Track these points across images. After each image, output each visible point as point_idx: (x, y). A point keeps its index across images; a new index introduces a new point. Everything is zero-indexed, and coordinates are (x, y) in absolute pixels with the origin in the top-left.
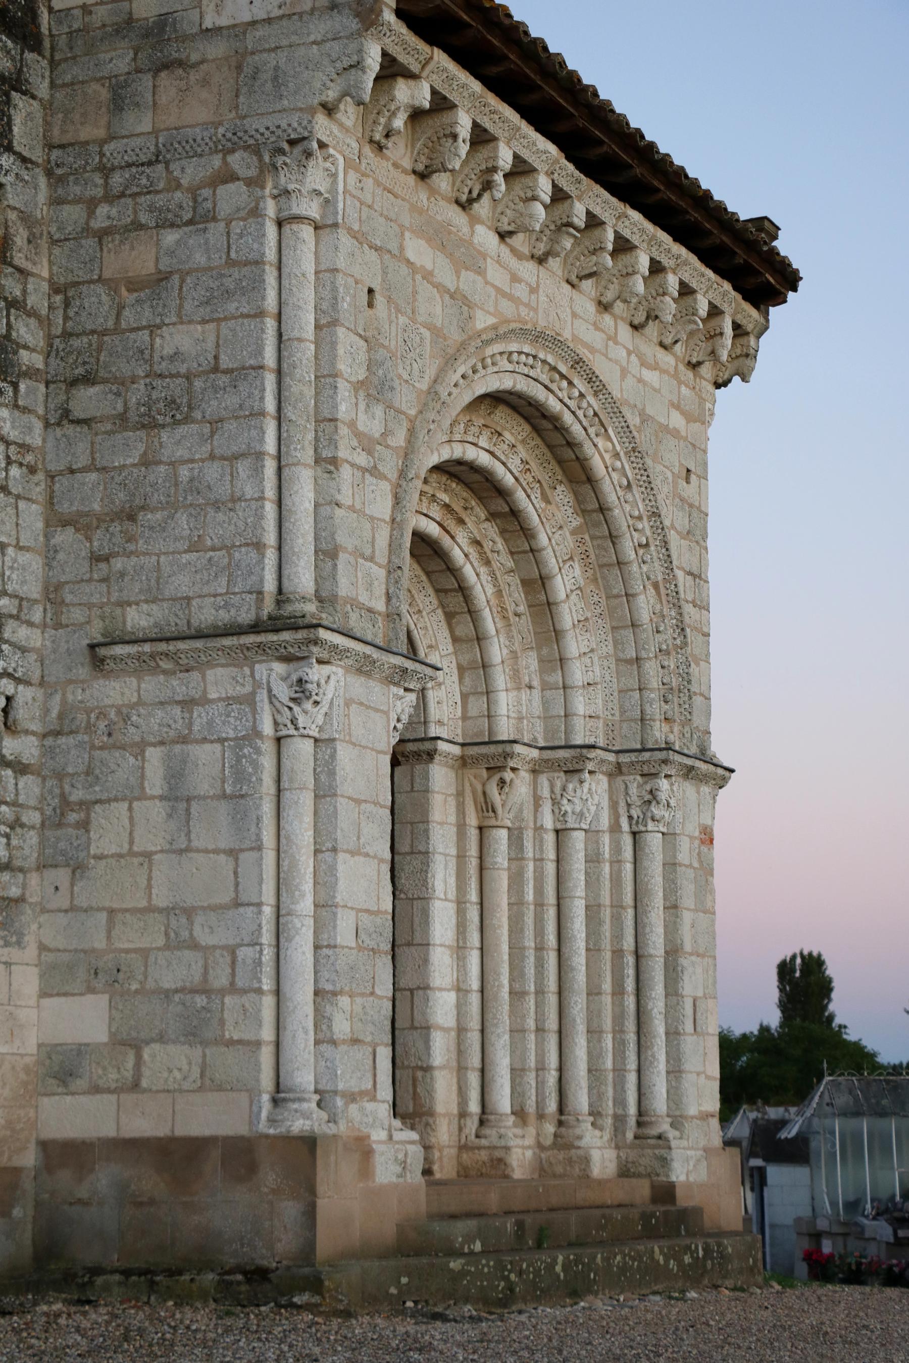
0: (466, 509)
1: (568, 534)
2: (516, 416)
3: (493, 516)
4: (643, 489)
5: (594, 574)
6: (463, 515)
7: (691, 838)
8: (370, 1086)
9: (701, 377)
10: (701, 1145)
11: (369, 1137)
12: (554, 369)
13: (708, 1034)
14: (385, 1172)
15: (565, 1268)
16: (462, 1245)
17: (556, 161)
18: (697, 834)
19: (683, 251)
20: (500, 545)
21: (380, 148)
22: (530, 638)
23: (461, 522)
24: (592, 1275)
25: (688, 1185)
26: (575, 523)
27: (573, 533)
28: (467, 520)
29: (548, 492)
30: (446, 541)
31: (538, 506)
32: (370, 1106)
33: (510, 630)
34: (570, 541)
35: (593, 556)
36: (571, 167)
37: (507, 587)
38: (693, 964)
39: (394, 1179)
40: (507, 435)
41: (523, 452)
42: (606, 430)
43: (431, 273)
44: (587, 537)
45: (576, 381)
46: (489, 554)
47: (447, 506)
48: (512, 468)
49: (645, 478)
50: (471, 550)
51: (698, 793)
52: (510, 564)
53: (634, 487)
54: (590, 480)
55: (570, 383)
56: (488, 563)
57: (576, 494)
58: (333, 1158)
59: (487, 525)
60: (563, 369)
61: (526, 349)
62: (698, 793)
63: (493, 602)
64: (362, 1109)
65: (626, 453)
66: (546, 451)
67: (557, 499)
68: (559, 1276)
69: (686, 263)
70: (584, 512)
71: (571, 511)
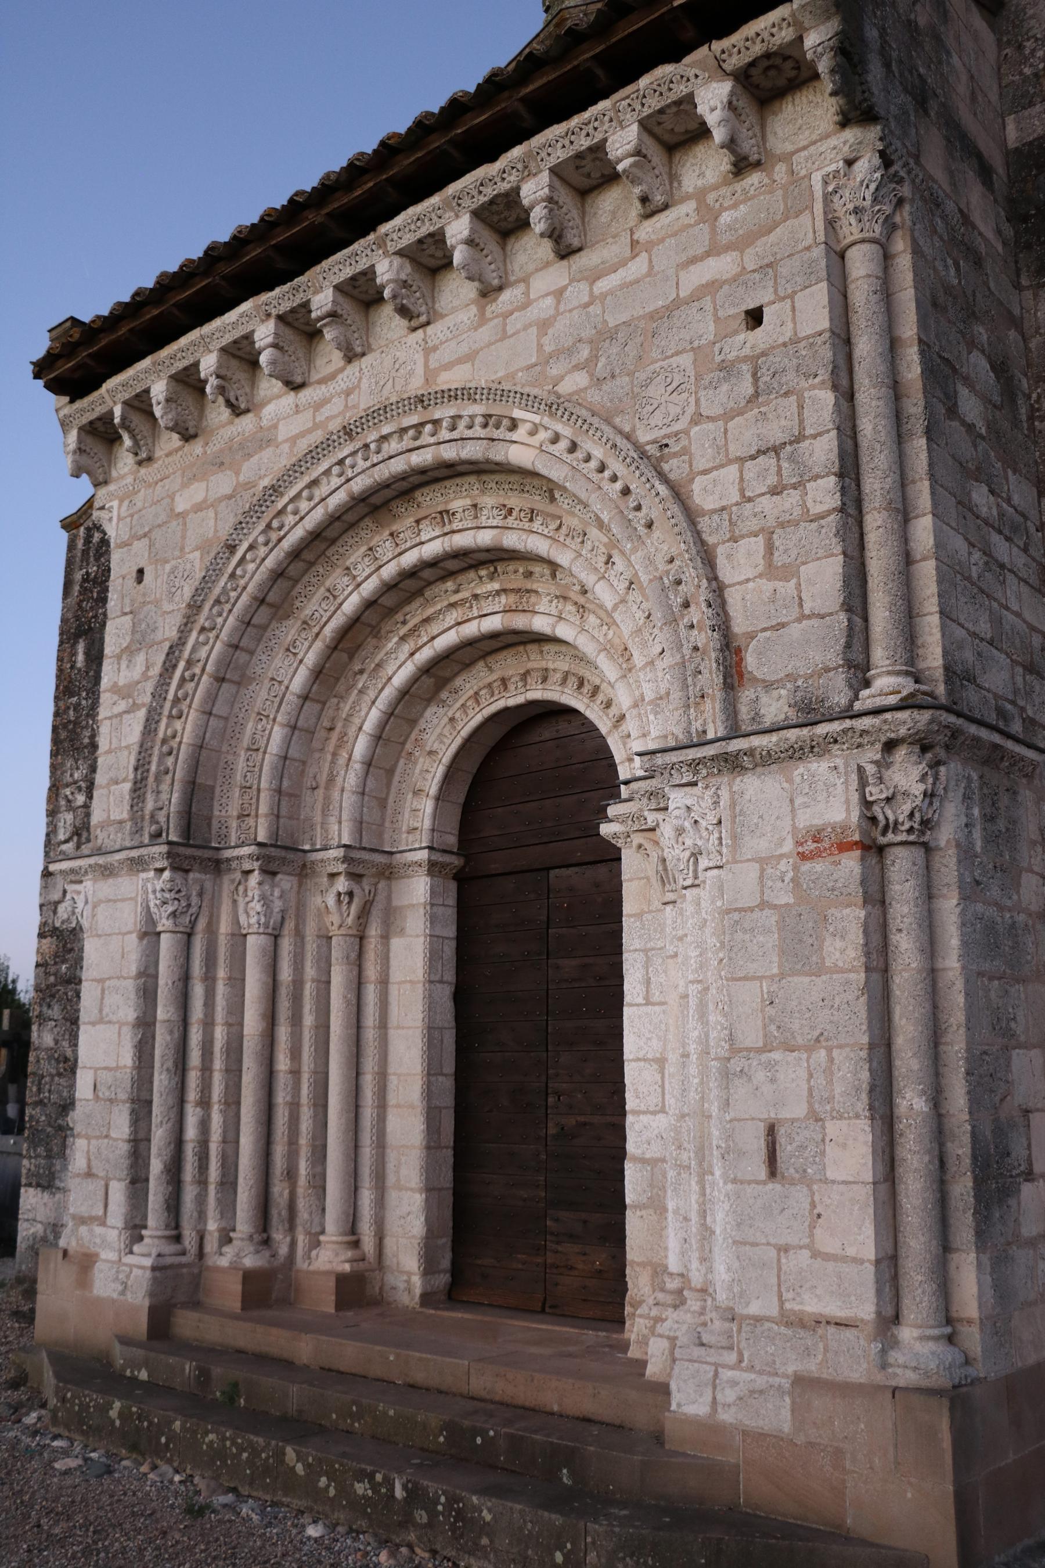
7: (763, 862)
8: (101, 1213)
9: (786, 158)
10: (791, 1369)
11: (97, 1255)
12: (404, 430)
13: (826, 1181)
14: (104, 1284)
15: (121, 1415)
16: (124, 1368)
17: (257, 307)
18: (788, 846)
19: (517, 152)
21: (149, 459)
24: (163, 1440)
25: (710, 1430)
28: (535, 587)
29: (551, 509)
30: (519, 622)
32: (98, 1230)
36: (278, 291)
38: (770, 1066)
39: (115, 1296)
40: (457, 504)
41: (488, 501)
42: (513, 420)
43: (205, 501)
51: (790, 781)
55: (436, 422)
58: (52, 1265)
61: (346, 452)
62: (790, 781)
64: (91, 1231)
67: (565, 506)
68: (113, 1422)
69: (529, 155)
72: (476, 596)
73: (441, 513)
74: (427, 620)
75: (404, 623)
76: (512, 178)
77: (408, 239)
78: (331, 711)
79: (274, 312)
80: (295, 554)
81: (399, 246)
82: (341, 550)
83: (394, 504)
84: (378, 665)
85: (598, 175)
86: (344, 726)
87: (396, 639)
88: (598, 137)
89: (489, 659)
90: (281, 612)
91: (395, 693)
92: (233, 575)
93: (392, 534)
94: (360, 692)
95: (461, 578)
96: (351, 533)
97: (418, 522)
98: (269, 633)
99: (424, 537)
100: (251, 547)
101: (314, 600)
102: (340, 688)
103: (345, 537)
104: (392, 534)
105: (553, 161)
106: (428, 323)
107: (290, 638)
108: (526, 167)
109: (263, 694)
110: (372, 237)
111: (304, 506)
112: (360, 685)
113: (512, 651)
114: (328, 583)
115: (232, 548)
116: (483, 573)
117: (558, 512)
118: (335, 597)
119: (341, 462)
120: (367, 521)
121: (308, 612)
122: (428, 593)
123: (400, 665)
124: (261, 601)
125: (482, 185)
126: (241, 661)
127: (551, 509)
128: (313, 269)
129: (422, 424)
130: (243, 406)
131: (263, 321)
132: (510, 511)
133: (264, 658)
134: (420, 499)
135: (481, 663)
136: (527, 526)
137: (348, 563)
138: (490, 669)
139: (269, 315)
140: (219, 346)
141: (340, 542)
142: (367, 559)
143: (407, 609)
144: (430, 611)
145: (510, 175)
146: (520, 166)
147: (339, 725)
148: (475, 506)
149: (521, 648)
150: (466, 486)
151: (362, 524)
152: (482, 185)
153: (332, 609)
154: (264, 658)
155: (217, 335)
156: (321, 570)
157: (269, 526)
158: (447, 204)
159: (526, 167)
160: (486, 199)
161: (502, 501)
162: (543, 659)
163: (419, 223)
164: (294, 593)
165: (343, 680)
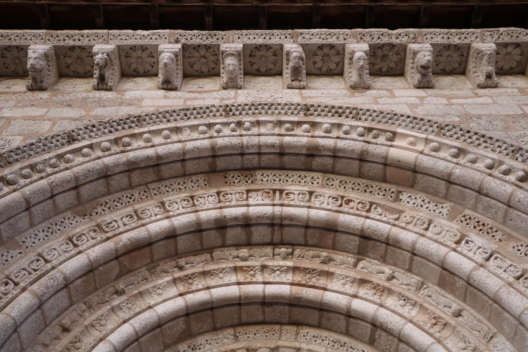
0: (324, 262)
1: (444, 222)
2: (290, 173)
3: (361, 253)
4: (484, 144)
5: (504, 233)
6: (325, 268)
12: (280, 123)
20: (387, 270)
22: (487, 326)
23: (329, 275)
26: (445, 211)
27: (451, 218)
28: (332, 270)
31: (385, 219)
33: (458, 332)
34: (455, 226)
35: (489, 222)
37: (428, 299)
41: (328, 192)
42: (394, 134)
44: (468, 212)
45: (318, 120)
46: (387, 284)
47: (295, 269)
48: (324, 206)
49: (475, 137)
50: (363, 292)
52: (415, 279)
53: (470, 148)
54: (415, 170)
55: (314, 125)
56: (390, 292)
57: (425, 190)
59: (361, 264)
60: (295, 119)
63: (422, 318)
65: (438, 134)
66: (359, 180)
69: (420, 34)
70: (446, 197)
71: (432, 206)
72: (264, 268)
73: (274, 191)
74: (205, 274)
75: (181, 268)
76: (403, 40)
77: (316, 40)
78: (74, 314)
79: (183, 41)
80: (132, 167)
81: (307, 42)
82: (163, 189)
83: (232, 174)
84: (141, 294)
85: (442, 67)
86: (82, 332)
87: (170, 278)
88: (467, 41)
89: (240, 329)
90: (80, 208)
91: (155, 319)
92: (60, 157)
93: (218, 193)
94: (113, 309)
95: (256, 251)
96: (181, 180)
97: (248, 191)
98: (58, 218)
99: (251, 201)
100: (91, 146)
101: (118, 213)
102: (94, 298)
103: (172, 181)
104: (218, 193)
105: (434, 41)
106: (304, 88)
107: (78, 230)
108: (414, 38)
109: (24, 263)
110: (290, 31)
111: (157, 140)
112: (116, 303)
113: (266, 328)
114: (137, 207)
115: (71, 138)
116: (283, 250)
117: (401, 208)
118: (139, 218)
119: (210, 126)
120: (201, 178)
121: (108, 218)
122: (217, 253)
123: (165, 299)
124: (76, 185)
125: (382, 35)
126: (20, 224)
127: (395, 205)
128: (234, 31)
129: (299, 124)
130: (109, 84)
131: (170, 42)
132: (348, 201)
133: (41, 235)
134: (259, 177)
135: (231, 331)
136: (364, 213)
137: (165, 199)
138: (236, 338)
139: (177, 42)
140: (119, 44)
141: (167, 182)
142: (185, 203)
143: (191, 259)
144: (211, 267)
145: (403, 37)
146: (412, 36)
147: (76, 331)
148: (311, 193)
149: (277, 327)
150: (308, 179)
151: (194, 178)
152: (382, 35)
153: (134, 225)
154: (41, 235)
155: (124, 37)
156: (136, 195)
157: (116, 141)
158: (354, 36)
159: (414, 38)
160: (382, 42)
161: (341, 194)
162: (296, 340)
163: (329, 36)
164: (102, 200)
165: (100, 292)
